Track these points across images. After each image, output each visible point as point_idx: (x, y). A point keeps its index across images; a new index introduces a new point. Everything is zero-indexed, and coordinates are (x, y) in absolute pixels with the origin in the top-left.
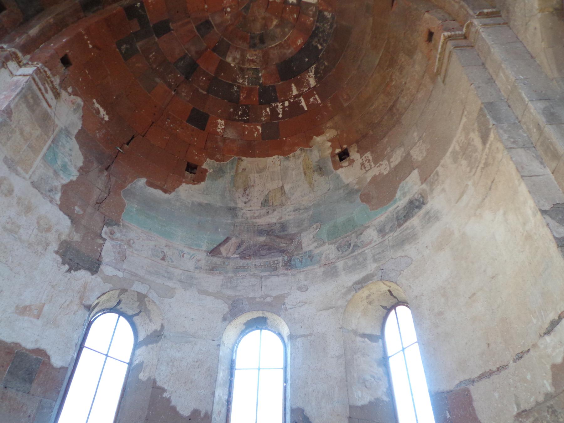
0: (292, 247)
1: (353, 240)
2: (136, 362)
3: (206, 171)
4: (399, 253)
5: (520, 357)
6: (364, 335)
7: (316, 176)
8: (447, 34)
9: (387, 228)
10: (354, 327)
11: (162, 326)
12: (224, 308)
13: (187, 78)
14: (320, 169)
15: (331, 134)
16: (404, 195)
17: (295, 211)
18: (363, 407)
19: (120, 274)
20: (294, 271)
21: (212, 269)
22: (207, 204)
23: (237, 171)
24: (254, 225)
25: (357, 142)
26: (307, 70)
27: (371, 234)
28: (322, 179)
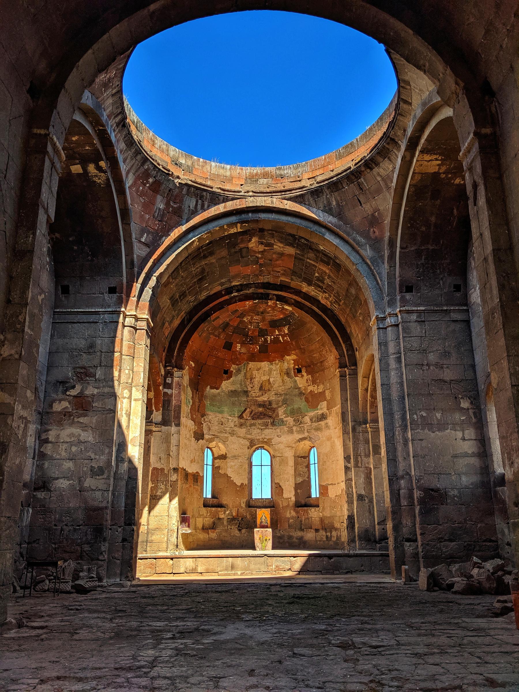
0: (274, 415)
2: (216, 465)
3: (232, 371)
4: (316, 433)
7: (286, 377)
9: (314, 420)
13: (224, 330)
14: (288, 373)
17: (275, 395)
19: (210, 437)
20: (275, 427)
21: (241, 425)
23: (247, 369)
25: (306, 367)
26: (284, 326)
27: (307, 419)
28: (289, 379)
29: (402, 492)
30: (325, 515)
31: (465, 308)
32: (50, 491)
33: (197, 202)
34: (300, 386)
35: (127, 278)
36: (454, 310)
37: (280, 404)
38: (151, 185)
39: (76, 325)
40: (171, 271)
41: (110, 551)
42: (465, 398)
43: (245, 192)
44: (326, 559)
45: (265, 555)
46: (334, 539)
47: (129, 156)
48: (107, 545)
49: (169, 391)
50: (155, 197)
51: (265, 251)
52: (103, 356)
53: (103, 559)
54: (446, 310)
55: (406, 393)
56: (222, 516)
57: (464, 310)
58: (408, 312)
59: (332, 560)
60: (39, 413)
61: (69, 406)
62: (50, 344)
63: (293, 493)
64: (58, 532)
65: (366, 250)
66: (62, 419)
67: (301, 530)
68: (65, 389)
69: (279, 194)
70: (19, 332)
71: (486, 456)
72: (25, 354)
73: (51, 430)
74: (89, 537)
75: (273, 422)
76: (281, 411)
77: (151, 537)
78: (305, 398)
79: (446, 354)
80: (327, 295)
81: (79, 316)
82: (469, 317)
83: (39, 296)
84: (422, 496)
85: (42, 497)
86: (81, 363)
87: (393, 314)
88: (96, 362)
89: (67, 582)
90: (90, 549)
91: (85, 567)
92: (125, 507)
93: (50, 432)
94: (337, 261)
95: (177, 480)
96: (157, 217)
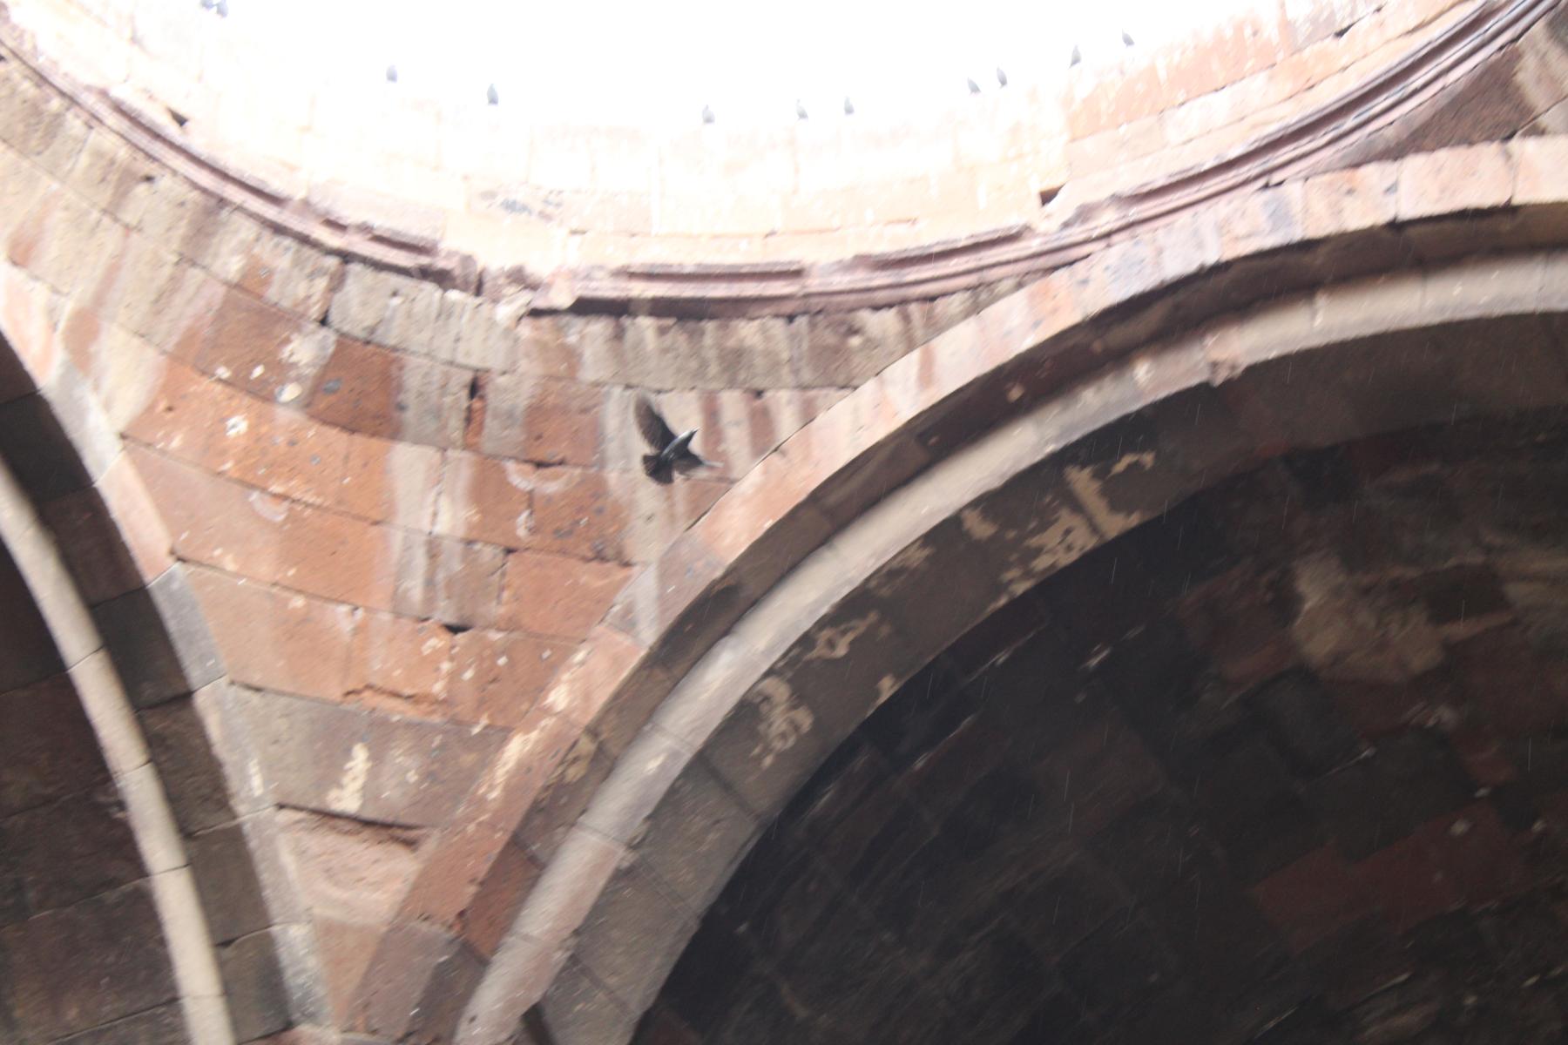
43: (1066, 225)
47: (58, 216)
51: (1456, 653)
69: (1322, 138)
96: (429, 600)
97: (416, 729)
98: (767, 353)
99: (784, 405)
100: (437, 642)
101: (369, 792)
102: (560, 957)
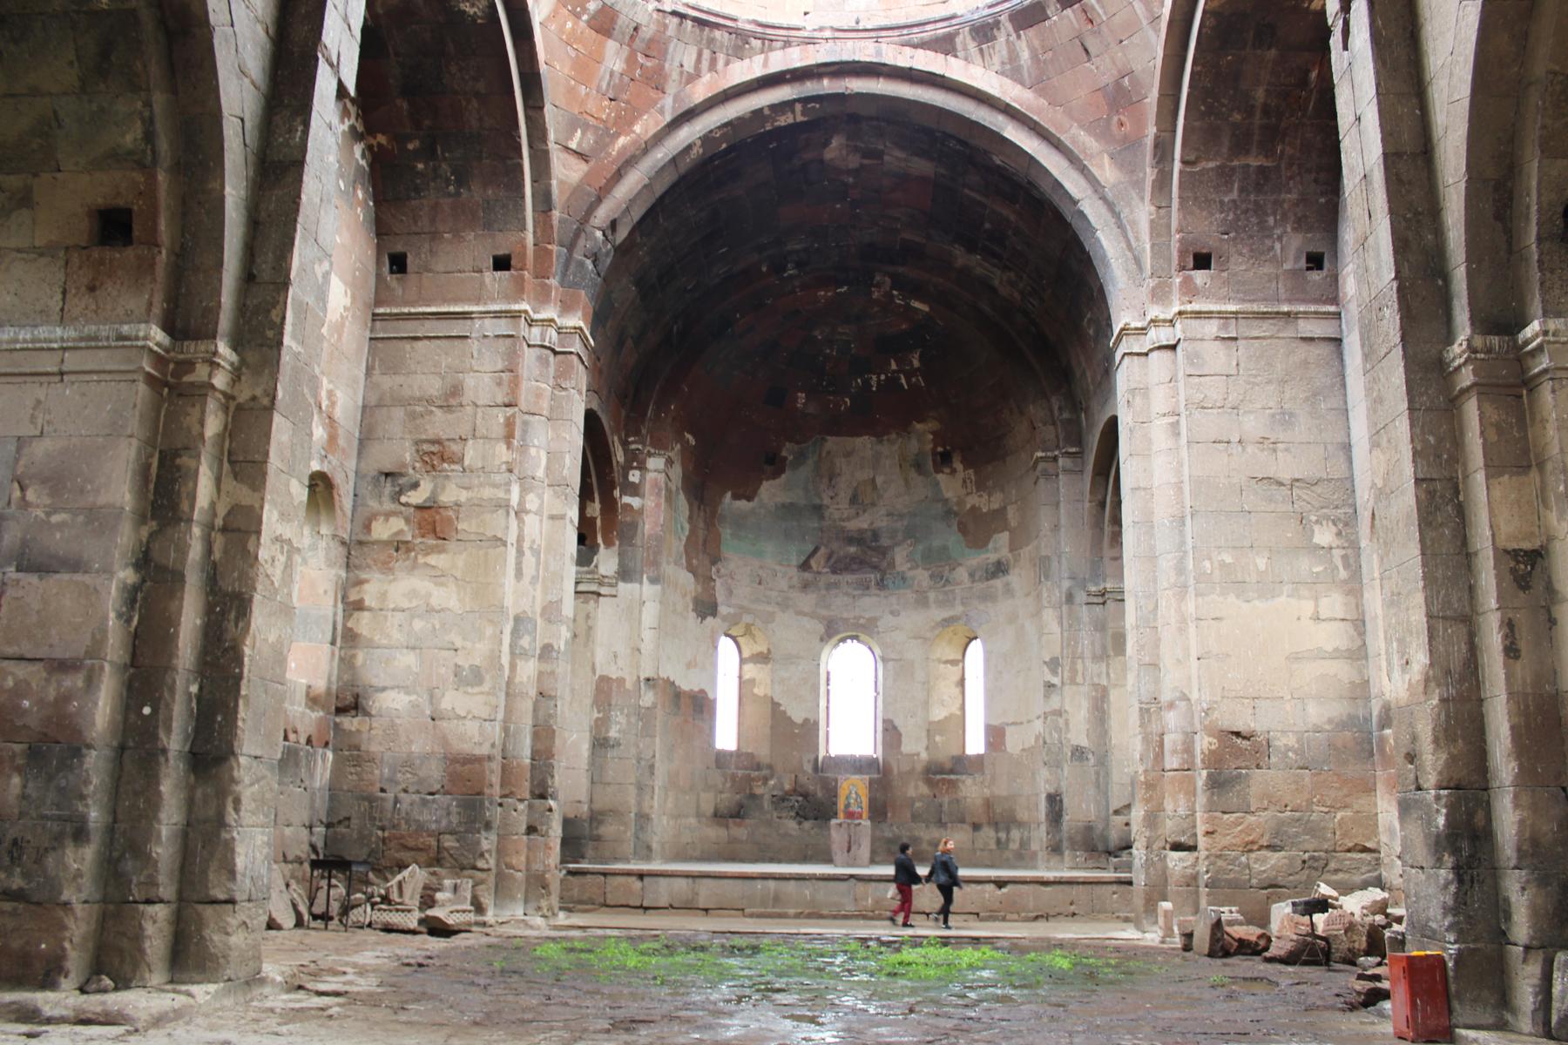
0: (884, 564)
1: (946, 574)
2: (747, 677)
3: (785, 459)
4: (981, 607)
5: (1029, 721)
6: (947, 662)
7: (913, 474)
8: (1040, 454)
9: (977, 578)
10: (938, 655)
11: (769, 650)
12: (821, 629)
15: (933, 425)
16: (996, 550)
17: (888, 515)
18: (939, 721)
19: (732, 610)
21: (805, 586)
22: (792, 504)
23: (820, 455)
24: (843, 530)
27: (962, 574)
29: (1166, 738)
30: (997, 792)
31: (1332, 309)
32: (367, 714)
33: (700, 55)
34: (949, 494)
35: (535, 232)
36: (1305, 313)
37: (900, 536)
38: (593, 18)
39: (420, 344)
40: (637, 214)
41: (501, 851)
42: (1324, 523)
44: (991, 887)
45: (852, 876)
46: (1014, 846)
48: (493, 837)
49: (635, 502)
50: (602, 46)
51: (862, 166)
52: (480, 415)
53: (485, 866)
54: (1288, 314)
55: (1189, 509)
56: (759, 791)
57: (1329, 313)
58: (1198, 315)
59: (1004, 890)
60: (343, 543)
61: (406, 528)
62: (365, 386)
63: (924, 742)
64: (389, 805)
65: (1101, 167)
66: (390, 556)
67: (941, 824)
68: (397, 489)
69: (896, 33)
70: (271, 347)
71: (1366, 657)
72: (284, 396)
73: (367, 581)
74: (455, 819)
75: (882, 580)
76: (900, 556)
77: (597, 828)
78: (960, 523)
79: (1285, 418)
80: (1012, 275)
81: (428, 324)
82: (1341, 330)
83: (316, 266)
84: (1213, 747)
85: (353, 729)
86: (430, 432)
87: (1164, 321)
88: (464, 430)
89: (409, 911)
90: (457, 845)
91: (448, 882)
92: (533, 759)
93: (366, 587)
94: (1034, 192)
95: (654, 706)
96: (607, 90)
97: (596, 128)
98: (722, 43)
99: (721, 58)
100: (606, 103)
101: (579, 144)
102: (624, 206)
